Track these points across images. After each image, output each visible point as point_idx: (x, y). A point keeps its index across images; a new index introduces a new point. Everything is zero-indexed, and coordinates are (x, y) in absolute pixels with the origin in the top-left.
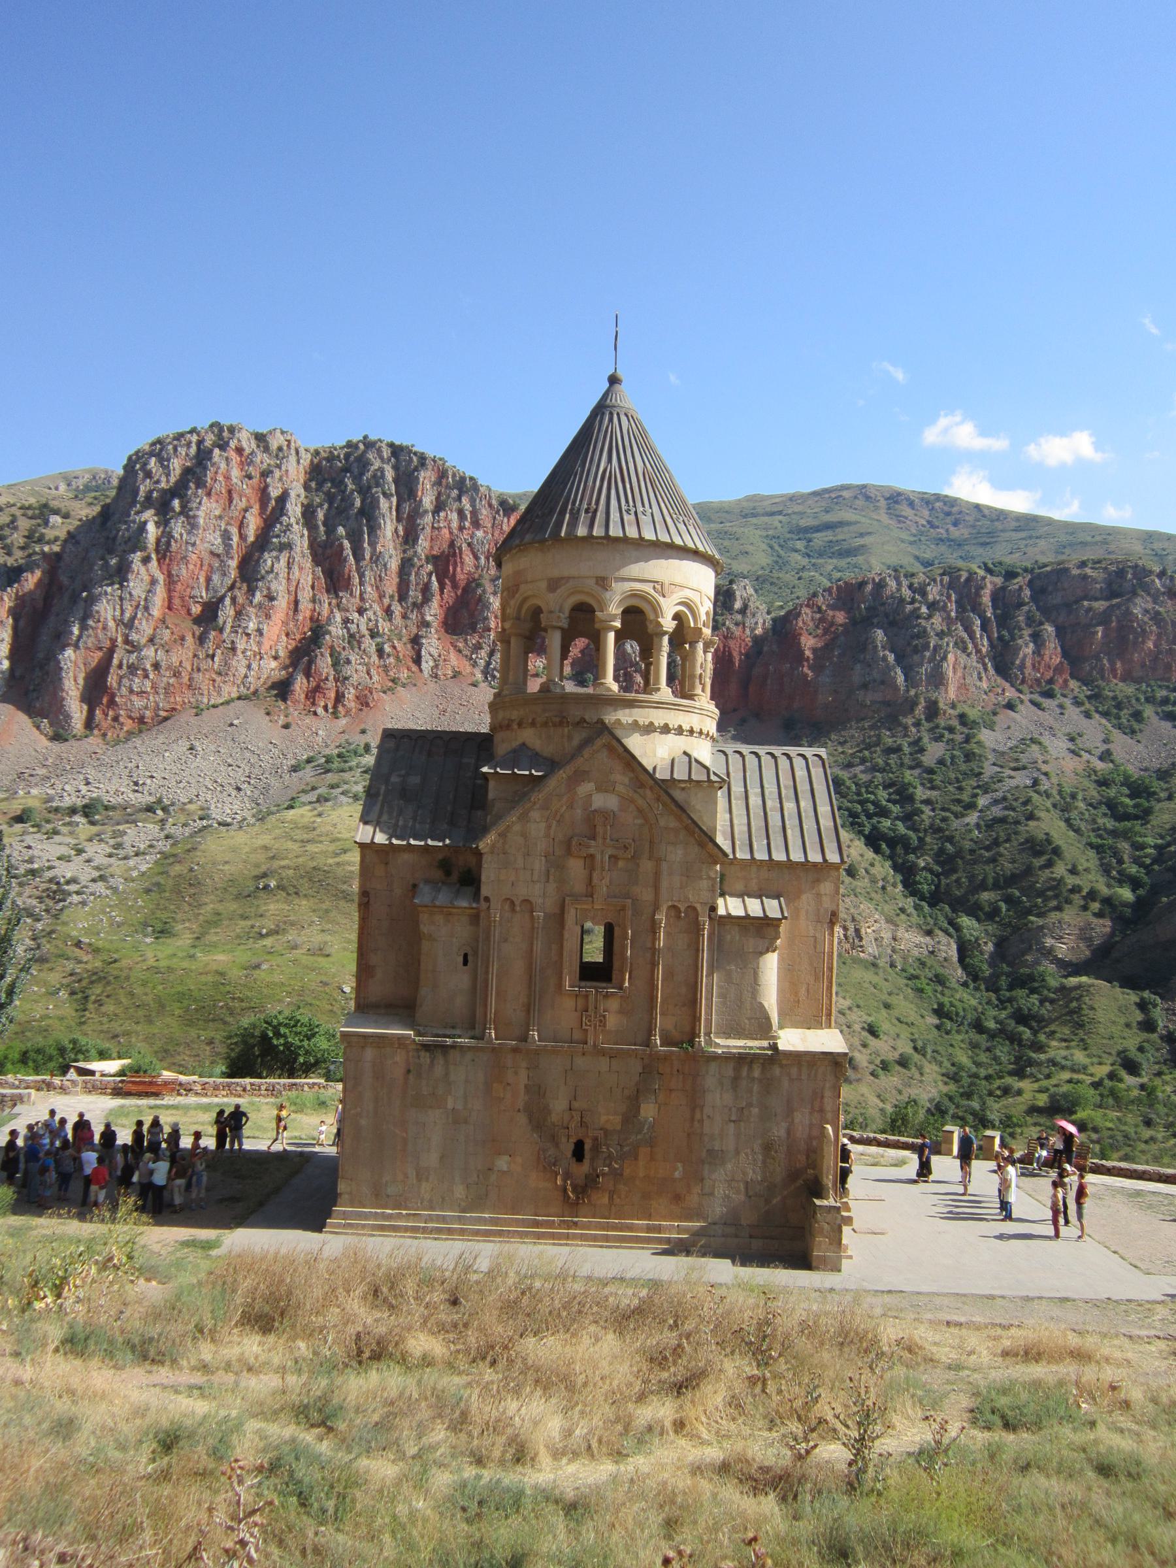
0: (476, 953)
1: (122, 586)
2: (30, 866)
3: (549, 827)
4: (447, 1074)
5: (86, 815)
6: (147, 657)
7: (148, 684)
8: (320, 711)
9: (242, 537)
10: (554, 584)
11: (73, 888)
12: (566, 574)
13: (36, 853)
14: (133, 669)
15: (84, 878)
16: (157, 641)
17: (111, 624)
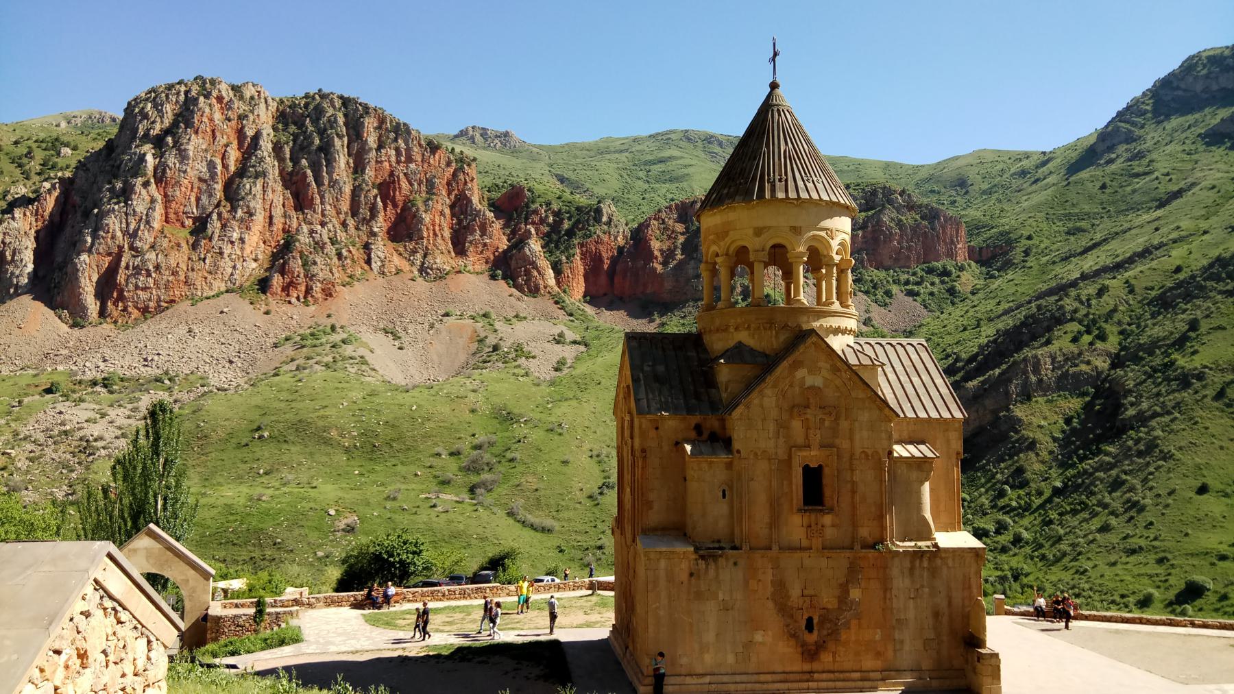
0: (731, 488)
1: (126, 204)
2: (63, 428)
3: (777, 401)
4: (717, 575)
5: (105, 386)
6: (149, 260)
7: (151, 281)
8: (294, 300)
9: (225, 167)
10: (758, 232)
11: (99, 444)
12: (768, 224)
13: (67, 417)
14: (137, 270)
15: (109, 436)
16: (157, 247)
17: (119, 234)
